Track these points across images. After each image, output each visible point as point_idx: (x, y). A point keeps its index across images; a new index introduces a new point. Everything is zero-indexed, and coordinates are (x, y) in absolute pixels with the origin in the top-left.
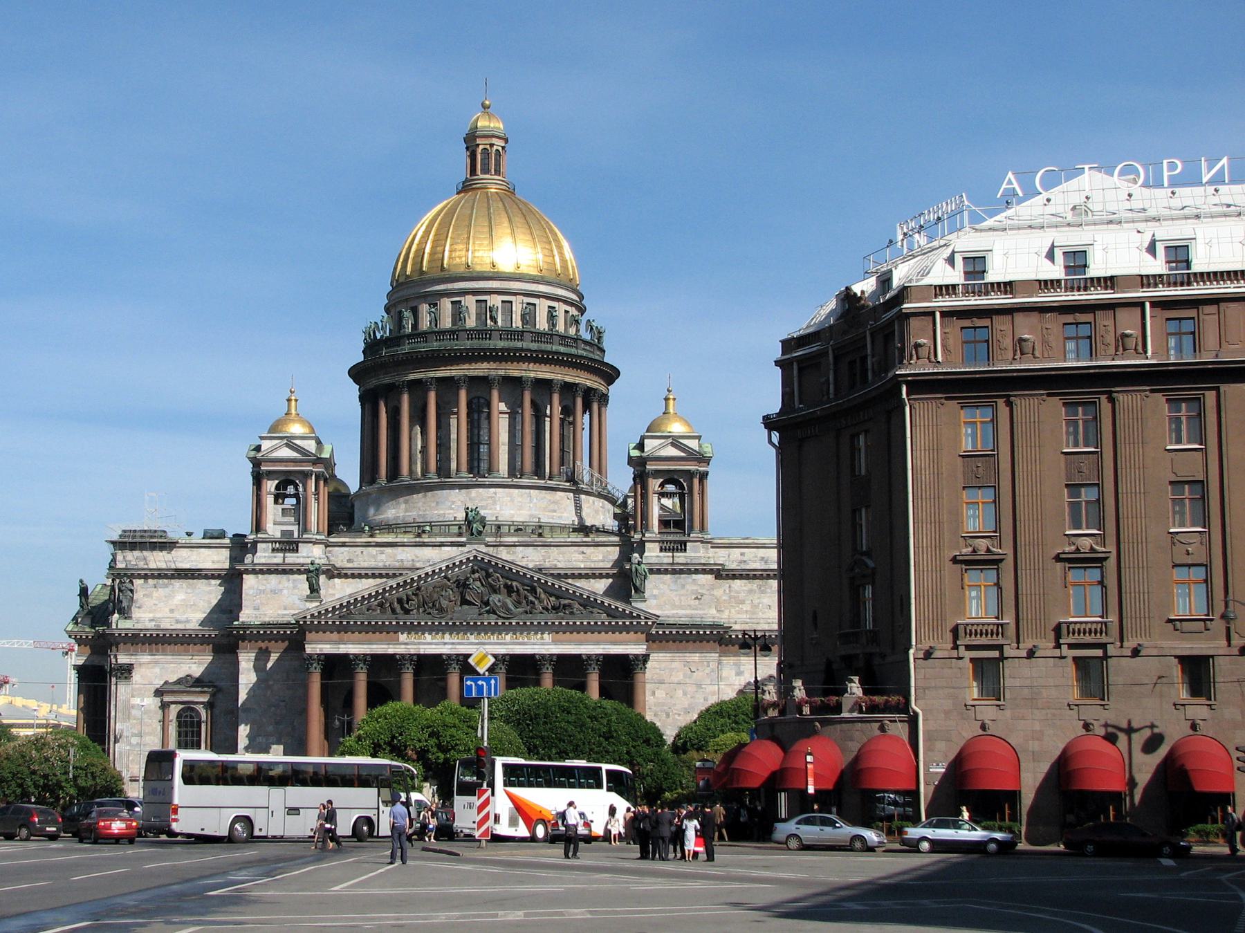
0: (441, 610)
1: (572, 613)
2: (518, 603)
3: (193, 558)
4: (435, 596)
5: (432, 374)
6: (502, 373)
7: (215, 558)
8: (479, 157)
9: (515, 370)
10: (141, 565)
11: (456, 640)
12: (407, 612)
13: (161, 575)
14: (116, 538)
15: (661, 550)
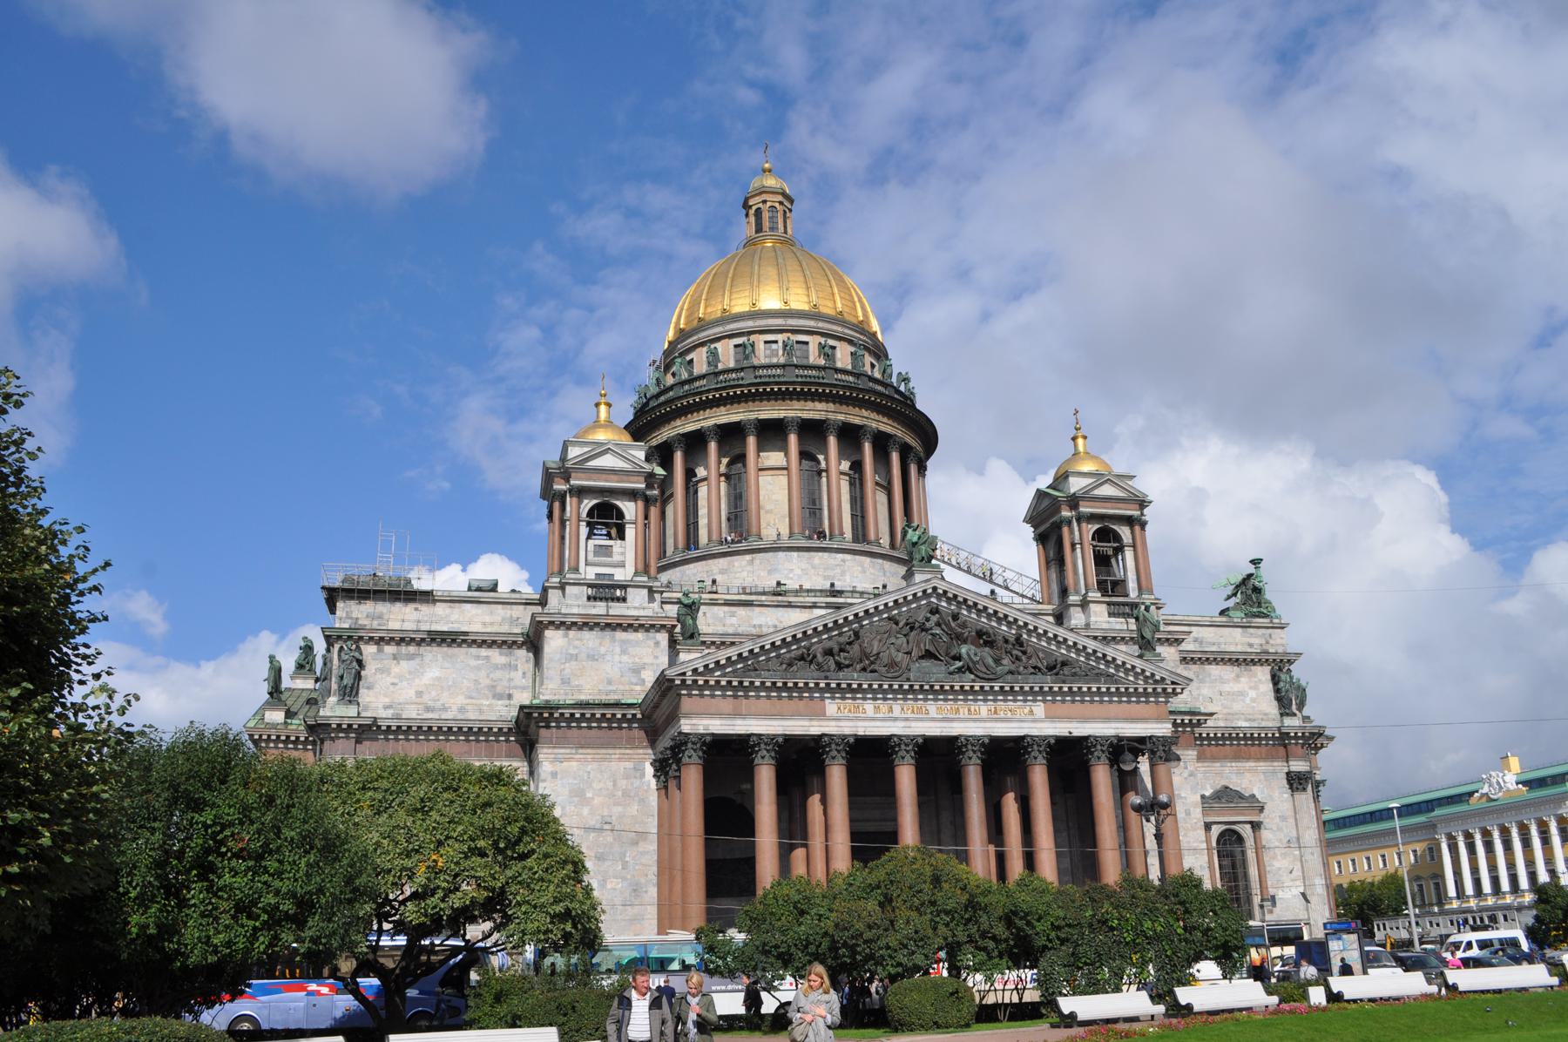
0: (892, 664)
1: (1074, 674)
2: (997, 661)
3: (455, 617)
4: (876, 643)
5: (753, 416)
6: (841, 417)
7: (488, 619)
8: (766, 215)
9: (856, 416)
10: (375, 624)
11: (909, 715)
12: (840, 667)
13: (402, 640)
14: (337, 584)
15: (1110, 615)
